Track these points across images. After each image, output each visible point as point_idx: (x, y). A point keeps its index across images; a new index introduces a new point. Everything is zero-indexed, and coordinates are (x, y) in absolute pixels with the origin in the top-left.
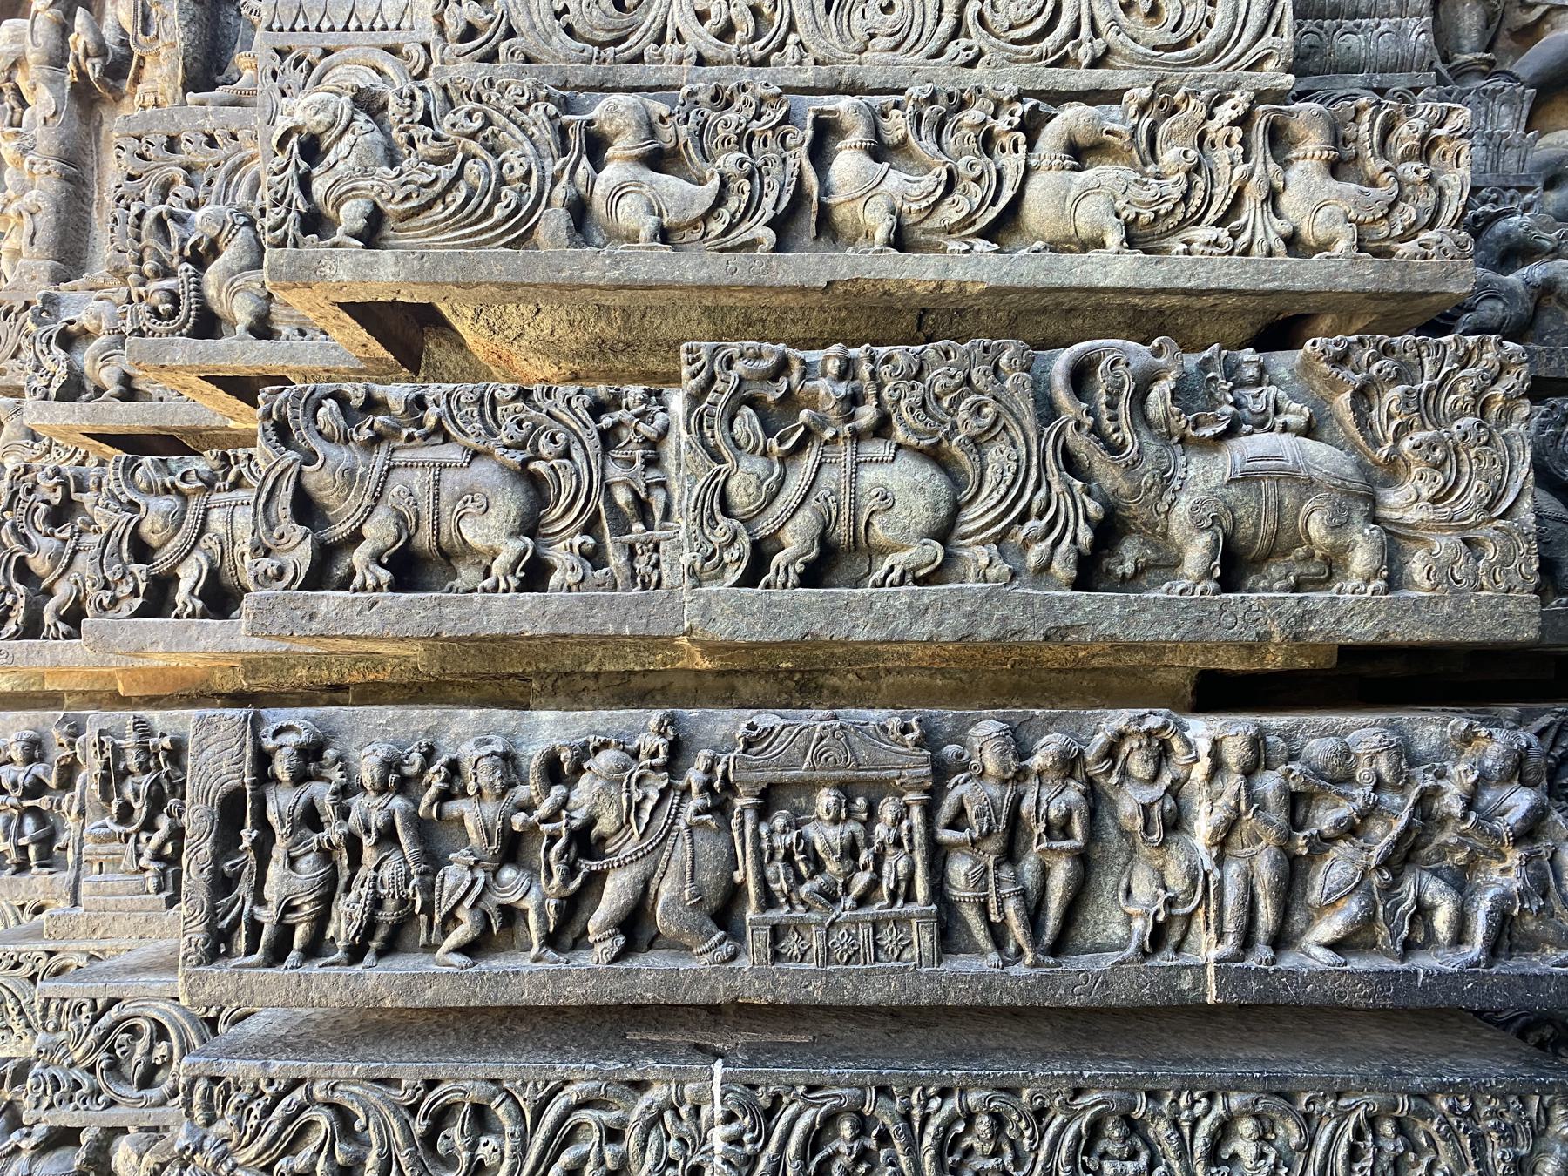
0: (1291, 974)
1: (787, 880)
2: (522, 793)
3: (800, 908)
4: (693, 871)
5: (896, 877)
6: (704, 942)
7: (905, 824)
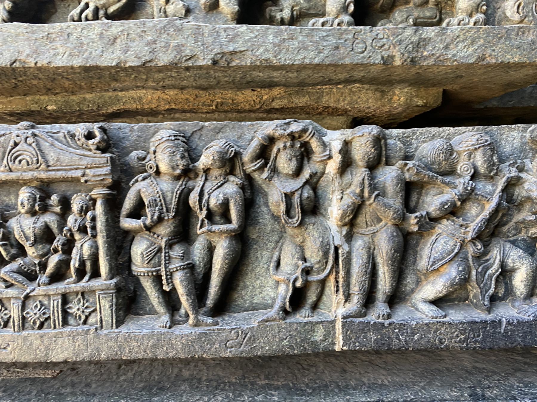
0: (403, 326)
7: (89, 214)
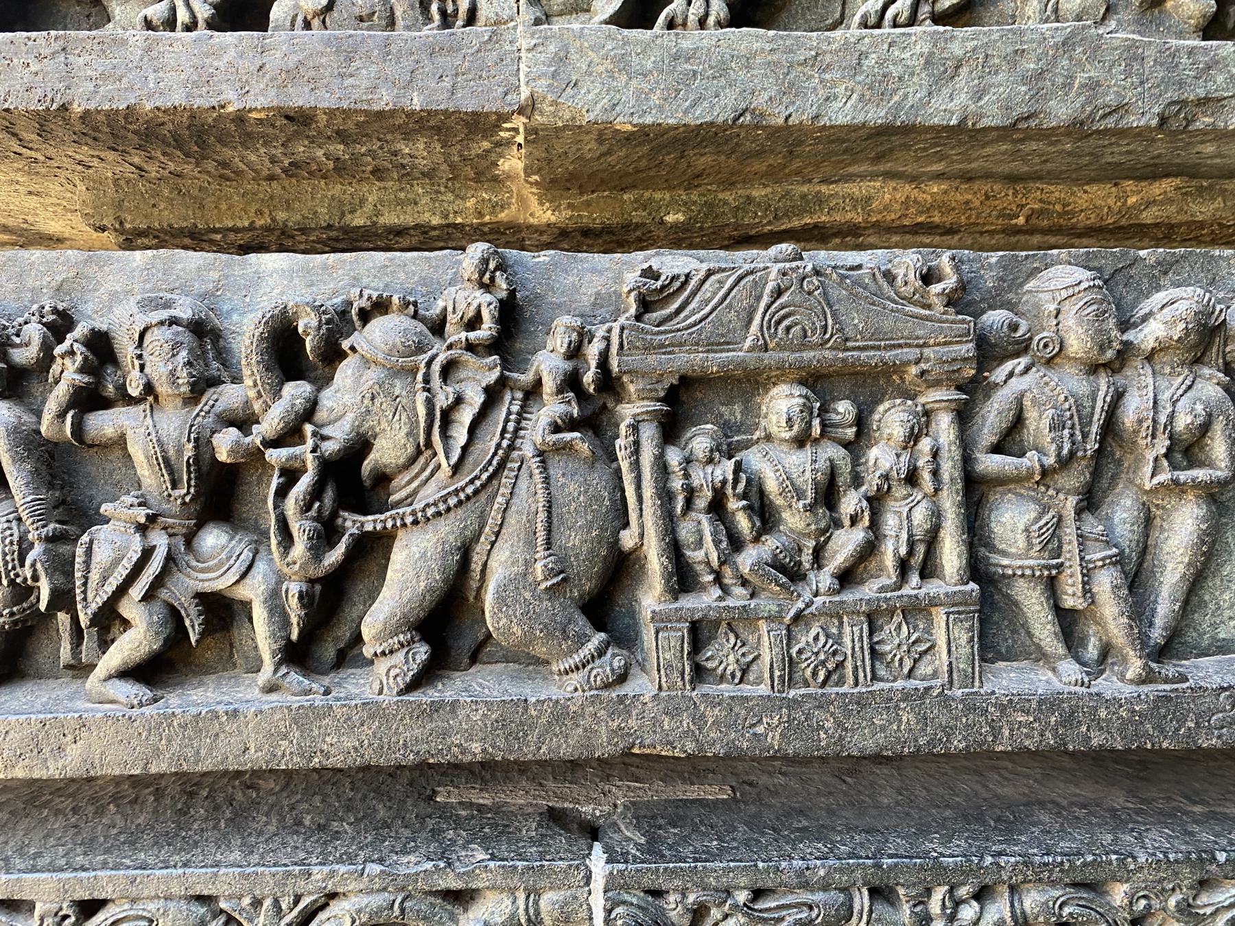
1: (717, 543)
2: (229, 396)
3: (739, 591)
4: (549, 530)
5: (910, 536)
6: (570, 652)
7: (925, 444)
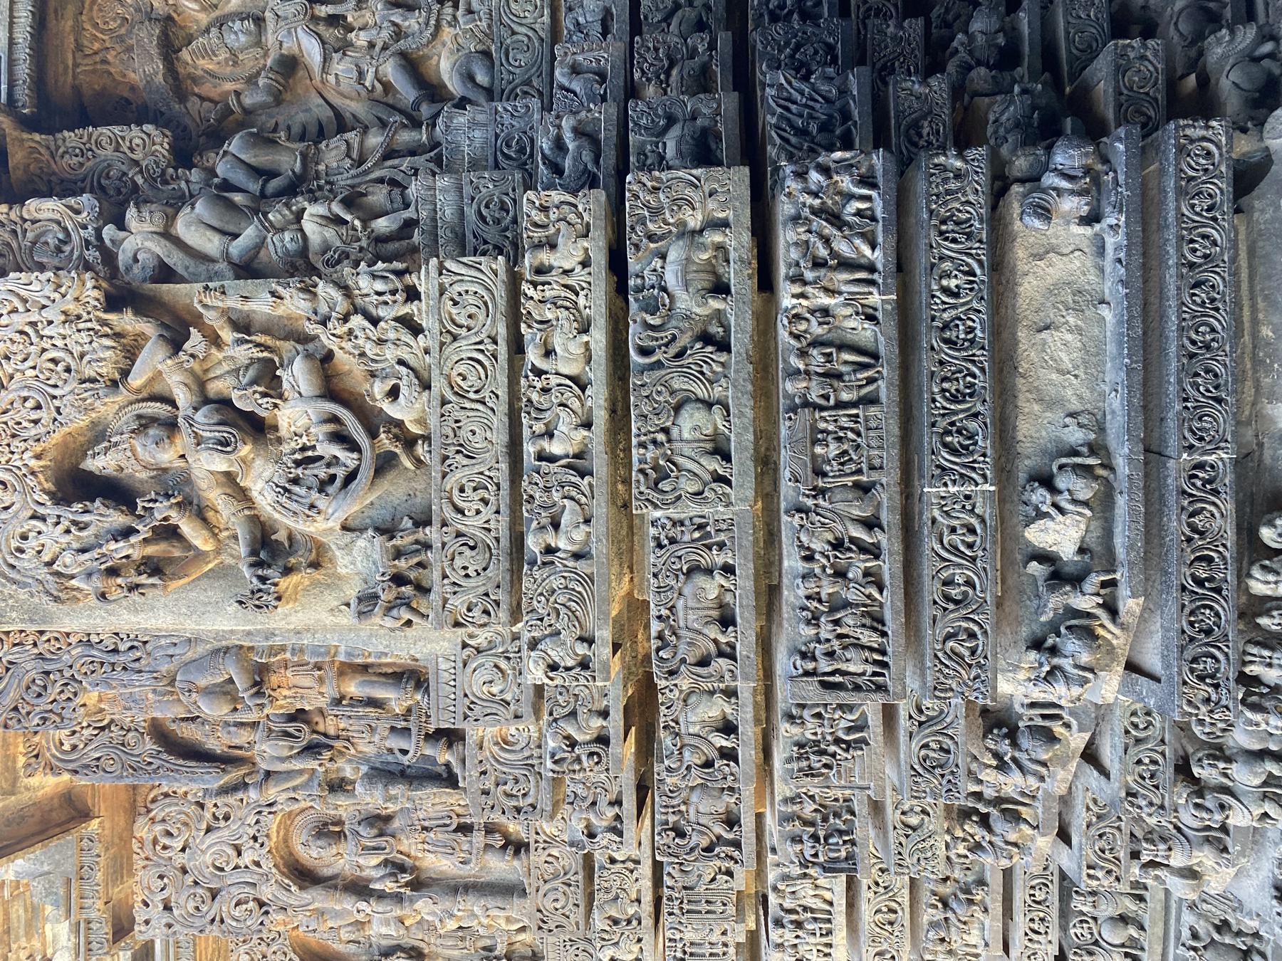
0: (884, 266)
2: (818, 571)
